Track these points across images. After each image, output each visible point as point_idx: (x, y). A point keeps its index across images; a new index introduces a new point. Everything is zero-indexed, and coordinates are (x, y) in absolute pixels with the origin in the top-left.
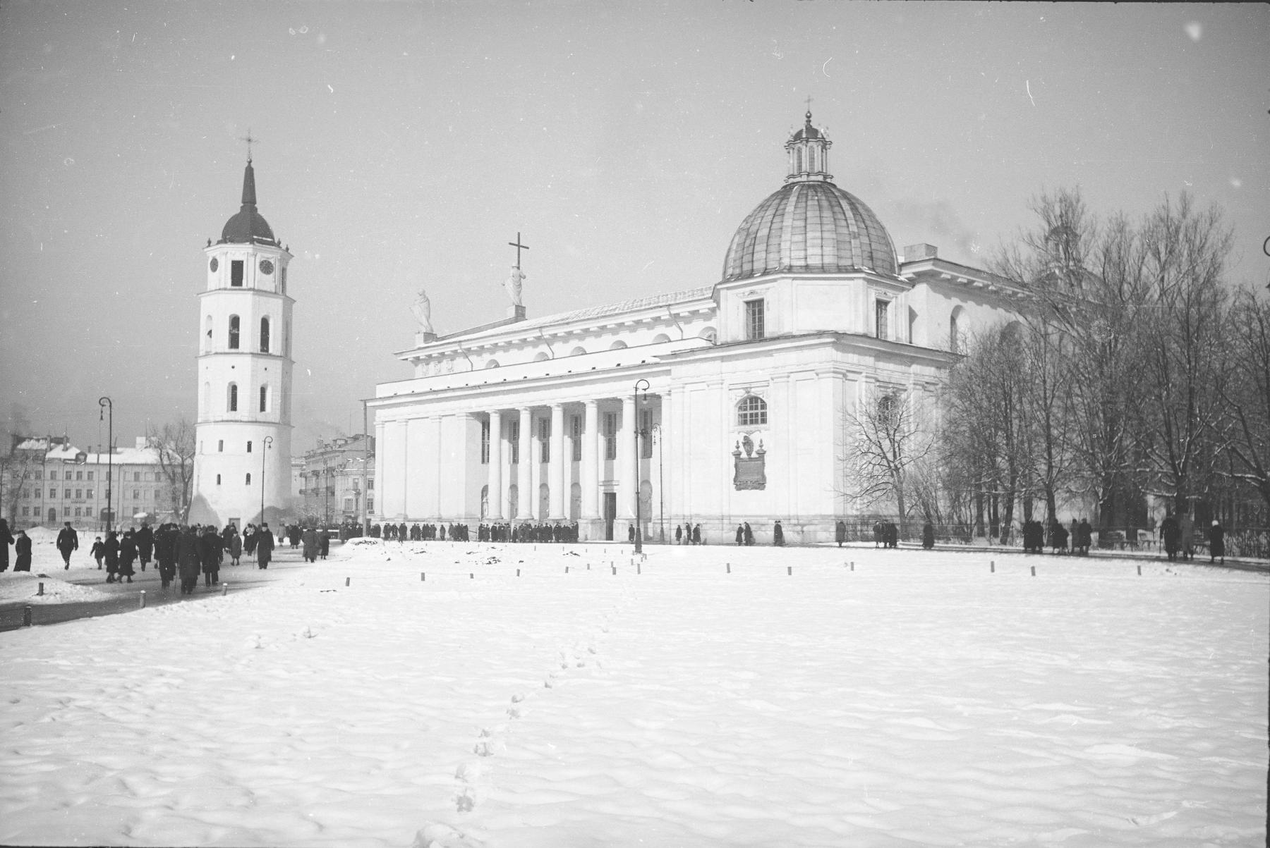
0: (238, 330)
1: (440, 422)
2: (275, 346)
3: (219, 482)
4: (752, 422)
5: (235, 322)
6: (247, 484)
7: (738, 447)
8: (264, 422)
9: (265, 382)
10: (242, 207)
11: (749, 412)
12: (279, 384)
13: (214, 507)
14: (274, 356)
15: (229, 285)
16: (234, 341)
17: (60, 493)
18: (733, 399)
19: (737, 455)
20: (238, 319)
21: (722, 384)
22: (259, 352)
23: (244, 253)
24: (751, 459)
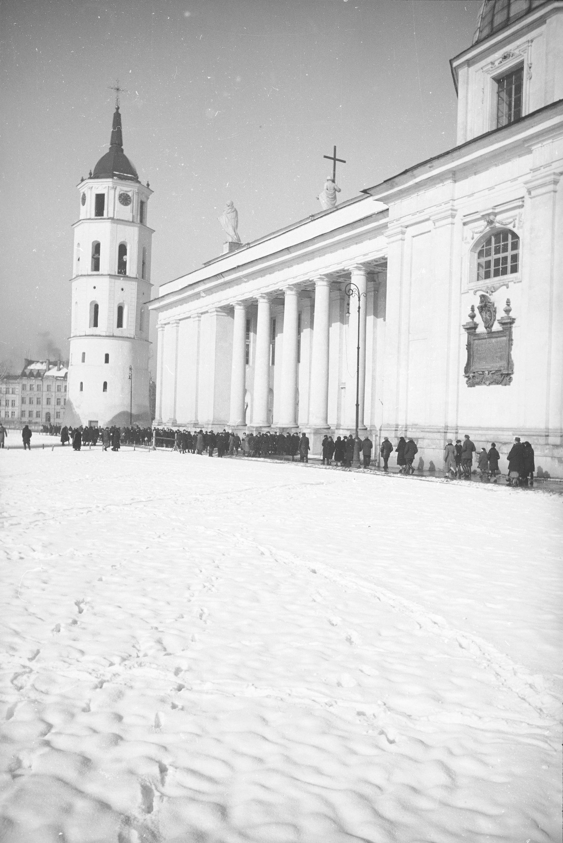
0: (99, 255)
1: (199, 320)
2: (132, 269)
3: (81, 389)
4: (497, 274)
5: (97, 248)
6: (104, 391)
7: (473, 317)
8: (119, 337)
9: (121, 301)
10: (110, 148)
11: (493, 257)
12: (134, 304)
13: (77, 411)
14: (130, 277)
15: (93, 215)
16: (96, 267)
17: (53, 401)
18: (469, 239)
19: (471, 329)
20: (100, 244)
21: (453, 216)
22: (117, 274)
23: (106, 187)
24: (491, 334)
